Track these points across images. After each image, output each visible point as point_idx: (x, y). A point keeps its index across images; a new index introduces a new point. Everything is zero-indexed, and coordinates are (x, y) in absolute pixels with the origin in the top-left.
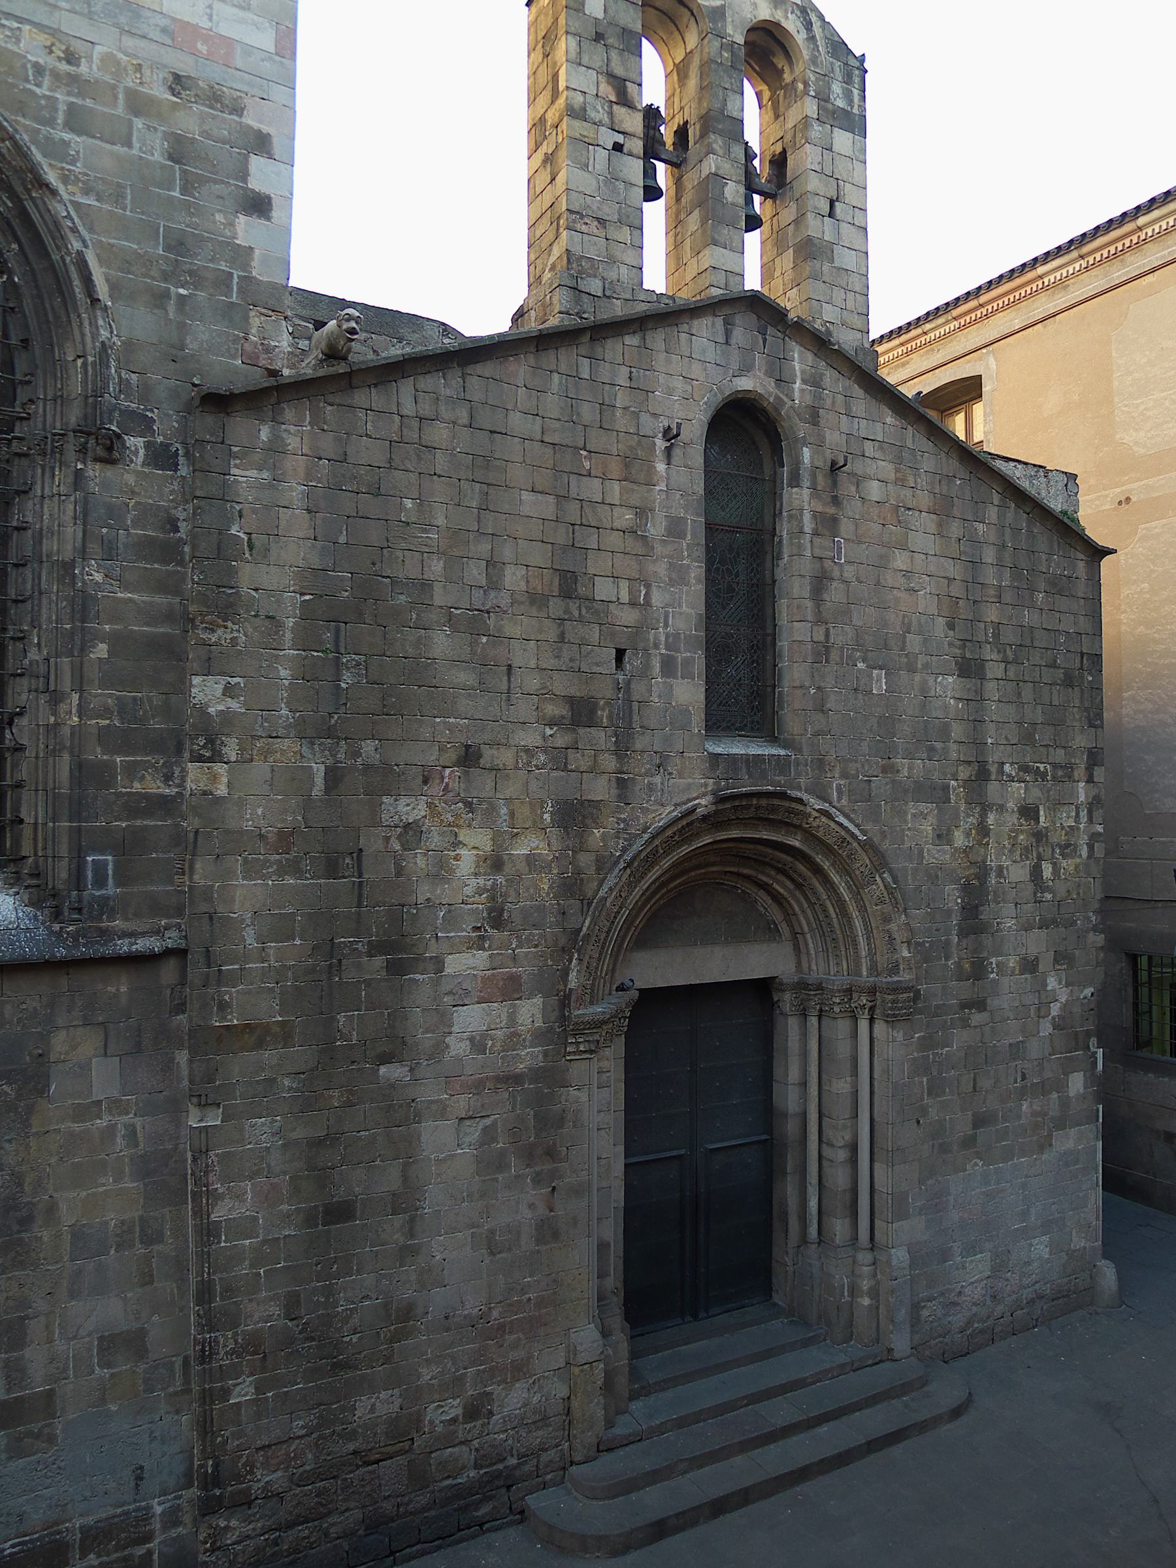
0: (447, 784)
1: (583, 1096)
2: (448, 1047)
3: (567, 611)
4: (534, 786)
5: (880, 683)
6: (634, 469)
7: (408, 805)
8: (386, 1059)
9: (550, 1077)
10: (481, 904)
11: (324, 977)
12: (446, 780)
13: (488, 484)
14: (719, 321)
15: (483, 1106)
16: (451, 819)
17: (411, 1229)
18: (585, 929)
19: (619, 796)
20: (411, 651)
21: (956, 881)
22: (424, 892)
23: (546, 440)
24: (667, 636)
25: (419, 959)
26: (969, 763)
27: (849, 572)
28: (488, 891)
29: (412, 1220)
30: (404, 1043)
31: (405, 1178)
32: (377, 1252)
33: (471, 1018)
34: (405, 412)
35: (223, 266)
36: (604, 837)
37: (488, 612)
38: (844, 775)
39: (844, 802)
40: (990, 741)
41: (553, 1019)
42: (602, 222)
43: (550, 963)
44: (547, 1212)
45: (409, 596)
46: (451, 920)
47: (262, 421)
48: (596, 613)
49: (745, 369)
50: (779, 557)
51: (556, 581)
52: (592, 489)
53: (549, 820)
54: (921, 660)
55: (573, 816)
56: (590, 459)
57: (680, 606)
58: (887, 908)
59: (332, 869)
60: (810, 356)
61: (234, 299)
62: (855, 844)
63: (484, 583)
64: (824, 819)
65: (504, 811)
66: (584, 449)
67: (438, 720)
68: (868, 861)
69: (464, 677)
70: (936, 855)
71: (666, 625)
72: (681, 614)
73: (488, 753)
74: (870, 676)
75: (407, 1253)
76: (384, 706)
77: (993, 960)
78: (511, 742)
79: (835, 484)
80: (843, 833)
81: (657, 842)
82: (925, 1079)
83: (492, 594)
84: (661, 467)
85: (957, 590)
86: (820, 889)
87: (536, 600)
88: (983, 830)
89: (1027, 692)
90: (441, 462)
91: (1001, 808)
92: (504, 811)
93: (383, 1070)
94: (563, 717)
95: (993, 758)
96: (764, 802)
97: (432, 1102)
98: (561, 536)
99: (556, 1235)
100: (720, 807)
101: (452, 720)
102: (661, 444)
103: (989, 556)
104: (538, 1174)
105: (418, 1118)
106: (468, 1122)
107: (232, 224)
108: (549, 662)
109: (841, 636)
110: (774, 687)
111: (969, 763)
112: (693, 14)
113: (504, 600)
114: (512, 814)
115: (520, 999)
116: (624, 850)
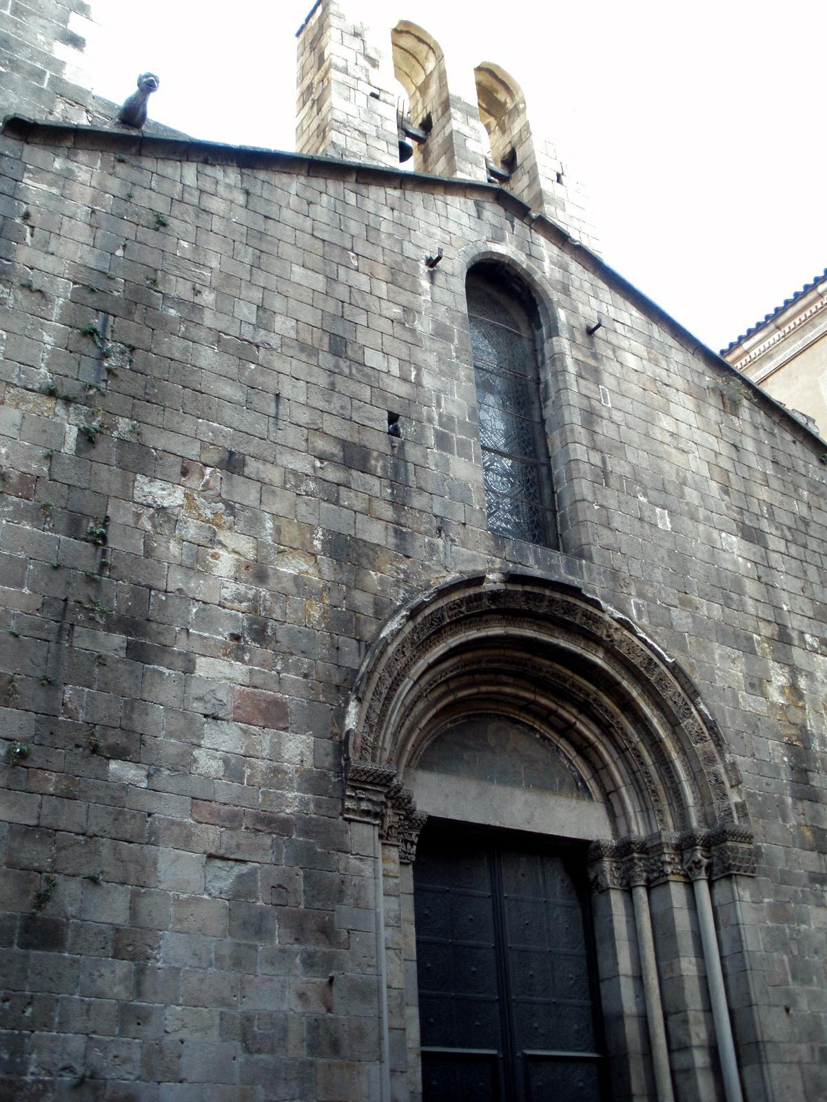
0: (208, 482)
1: (367, 869)
2: (195, 760)
3: (337, 366)
4: (302, 509)
5: (665, 522)
6: (399, 275)
7: (163, 489)
8: (120, 754)
10: (240, 617)
11: (52, 637)
12: (207, 477)
13: (261, 251)
14: (471, 203)
15: (238, 846)
16: (210, 516)
17: (138, 984)
18: (363, 669)
19: (397, 546)
20: (177, 355)
21: (779, 737)
22: (176, 580)
23: (316, 234)
24: (441, 415)
25: (165, 648)
27: (617, 416)
28: (249, 600)
29: (141, 971)
30: (142, 742)
31: (134, 911)
32: (90, 1004)
34: (187, 183)
35: (38, 65)
36: (382, 582)
37: (258, 347)
38: (640, 595)
39: (645, 621)
40: (785, 608)
41: (327, 764)
42: (363, 134)
43: (322, 698)
44: (323, 1010)
45: (179, 311)
46: (205, 619)
47: (57, 156)
48: (366, 375)
49: (498, 239)
50: (546, 399)
51: (326, 340)
52: (362, 281)
53: (319, 547)
54: (702, 513)
55: (346, 551)
56: (358, 260)
57: (452, 394)
58: (711, 746)
59: (74, 527)
60: (555, 250)
61: (45, 86)
62: (663, 667)
63: (254, 322)
64: (626, 632)
65: (269, 524)
66: (352, 250)
67: (200, 421)
68: (680, 690)
69: (228, 390)
70: (750, 703)
71: (439, 405)
72: (453, 401)
73: (252, 466)
74: (653, 511)
75: (131, 1017)
76: (146, 393)
78: (279, 461)
79: (592, 344)
80: (649, 652)
81: (441, 603)
83: (262, 332)
84: (425, 284)
85: (725, 464)
86: (630, 729)
87: (309, 350)
89: (812, 573)
90: (217, 224)
91: (810, 676)
92: (269, 524)
93: (114, 765)
94: (334, 455)
95: (794, 623)
96: (558, 596)
97: (173, 823)
98: (331, 307)
99: (335, 1047)
100: (511, 587)
101: (215, 425)
102: (423, 268)
103: (749, 445)
104: (311, 955)
105: (152, 840)
106: (219, 863)
107: (50, 44)
108: (322, 405)
109: (617, 466)
110: (554, 512)
112: (430, 48)
113: (275, 341)
114: (278, 530)
115: (285, 729)
116: (405, 601)
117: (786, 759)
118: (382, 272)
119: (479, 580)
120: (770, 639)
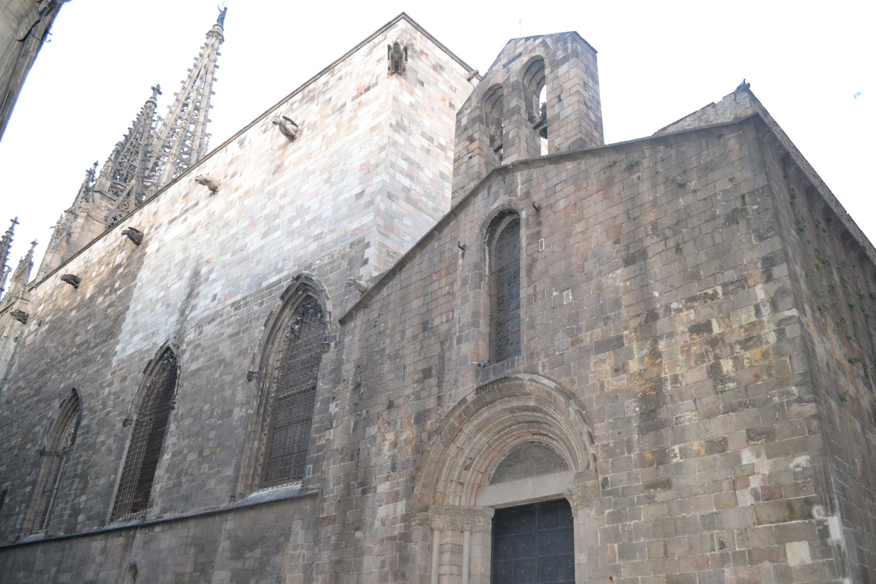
9: (406, 537)
26: (638, 315)
33: (383, 511)
70: (612, 383)
77: (676, 448)
82: (616, 546)
88: (655, 354)
111: (638, 315)
117: (637, 409)
118: (443, 273)
119: (464, 400)
120: (635, 330)
